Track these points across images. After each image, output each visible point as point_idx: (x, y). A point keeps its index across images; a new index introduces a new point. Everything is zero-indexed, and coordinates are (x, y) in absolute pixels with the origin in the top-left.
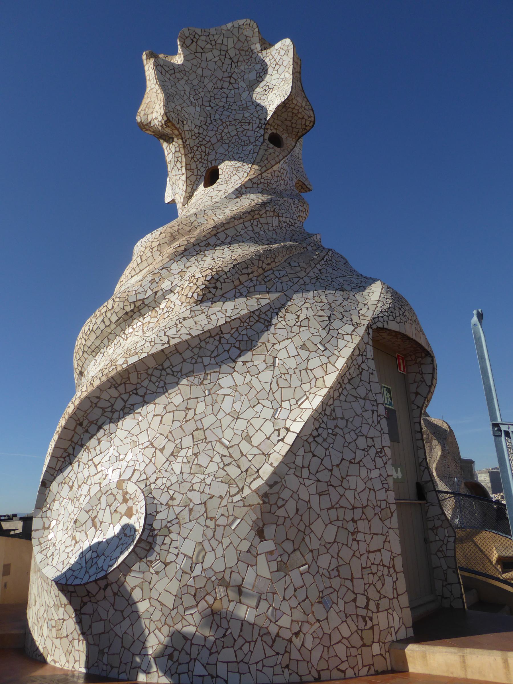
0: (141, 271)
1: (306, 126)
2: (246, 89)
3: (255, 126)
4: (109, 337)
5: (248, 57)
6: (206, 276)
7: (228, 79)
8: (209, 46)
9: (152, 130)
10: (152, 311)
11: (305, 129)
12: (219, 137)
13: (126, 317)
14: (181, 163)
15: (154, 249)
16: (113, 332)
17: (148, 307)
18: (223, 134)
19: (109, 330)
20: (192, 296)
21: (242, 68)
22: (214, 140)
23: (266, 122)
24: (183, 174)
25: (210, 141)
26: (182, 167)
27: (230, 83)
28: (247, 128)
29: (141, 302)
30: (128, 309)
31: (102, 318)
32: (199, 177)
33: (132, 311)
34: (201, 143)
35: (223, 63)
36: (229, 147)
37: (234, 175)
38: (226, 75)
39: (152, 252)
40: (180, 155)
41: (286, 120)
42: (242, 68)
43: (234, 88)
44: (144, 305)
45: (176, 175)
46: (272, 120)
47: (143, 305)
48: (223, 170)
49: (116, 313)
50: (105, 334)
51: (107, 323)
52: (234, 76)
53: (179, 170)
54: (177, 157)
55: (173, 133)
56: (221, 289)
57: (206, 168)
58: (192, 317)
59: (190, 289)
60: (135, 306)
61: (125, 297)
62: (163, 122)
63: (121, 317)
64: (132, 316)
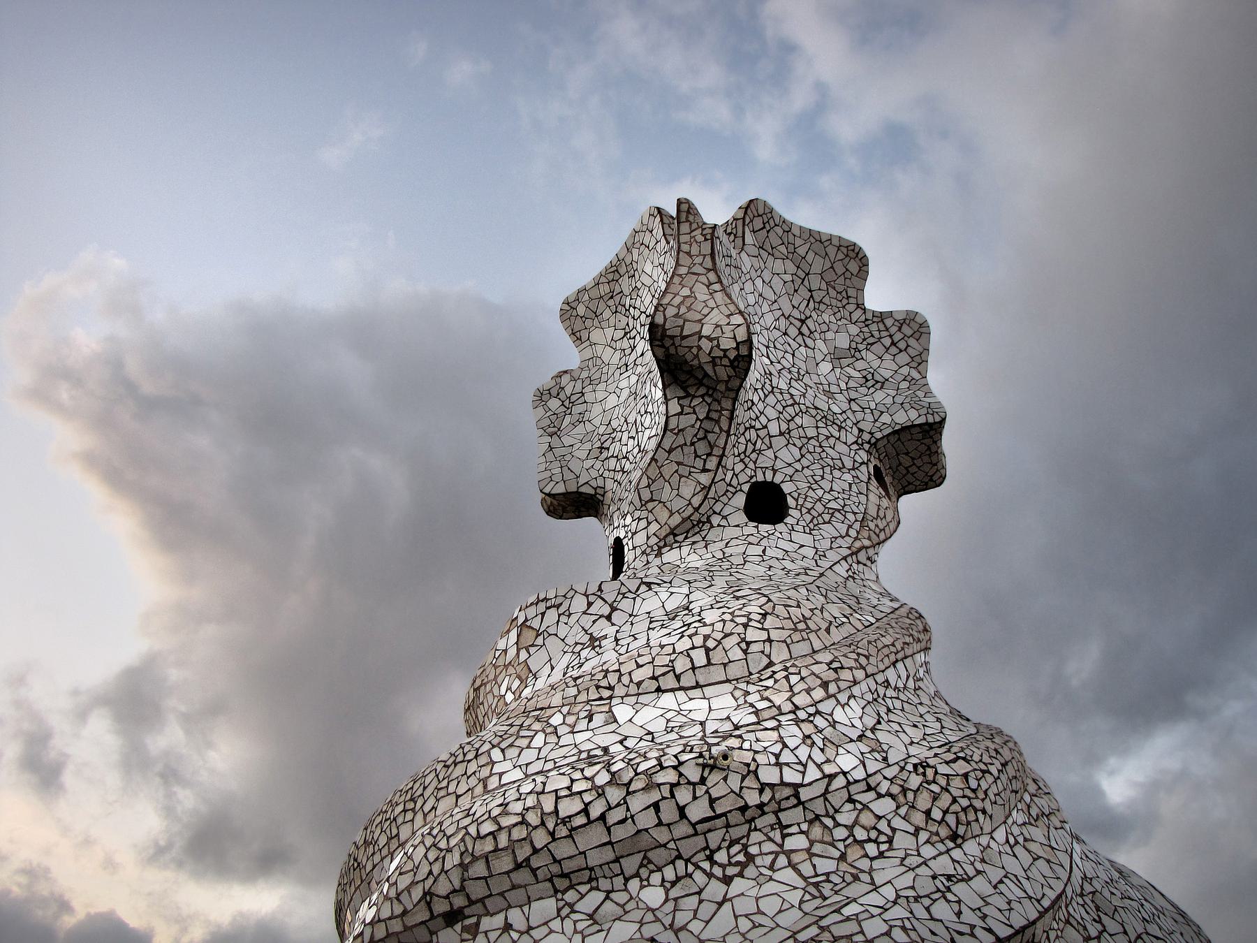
0: (698, 686)
1: (931, 480)
2: (828, 358)
3: (851, 439)
4: (650, 854)
5: (839, 305)
6: (966, 776)
7: (798, 324)
8: (783, 249)
9: (672, 351)
10: (811, 822)
11: (926, 484)
12: (784, 427)
13: (735, 818)
14: (712, 447)
15: (753, 648)
16: (672, 845)
17: (805, 808)
18: (792, 425)
19: (662, 835)
20: (943, 819)
21: (826, 317)
22: (774, 428)
23: (873, 441)
24: (704, 470)
25: (765, 427)
26: (709, 455)
27: (801, 333)
28: (836, 434)
29: (788, 792)
30: (753, 798)
31: (655, 796)
32: (732, 490)
33: (761, 806)
34: (753, 423)
35: (796, 291)
36: (803, 456)
37: (825, 523)
38: (796, 314)
39: (745, 652)
40: (717, 429)
41: (907, 454)
42: (826, 317)
43: (806, 346)
44: (795, 802)
45: (679, 464)
46: (885, 441)
47: (793, 801)
48: (797, 500)
49: (712, 801)
50: (645, 841)
51: (669, 812)
52: (809, 322)
53: (697, 456)
54: (707, 431)
55: (727, 382)
56: (991, 817)
57: (751, 477)
58: (963, 880)
59: (935, 799)
60: (773, 798)
61: (748, 765)
62: (732, 355)
63: (724, 814)
64: (753, 819)
